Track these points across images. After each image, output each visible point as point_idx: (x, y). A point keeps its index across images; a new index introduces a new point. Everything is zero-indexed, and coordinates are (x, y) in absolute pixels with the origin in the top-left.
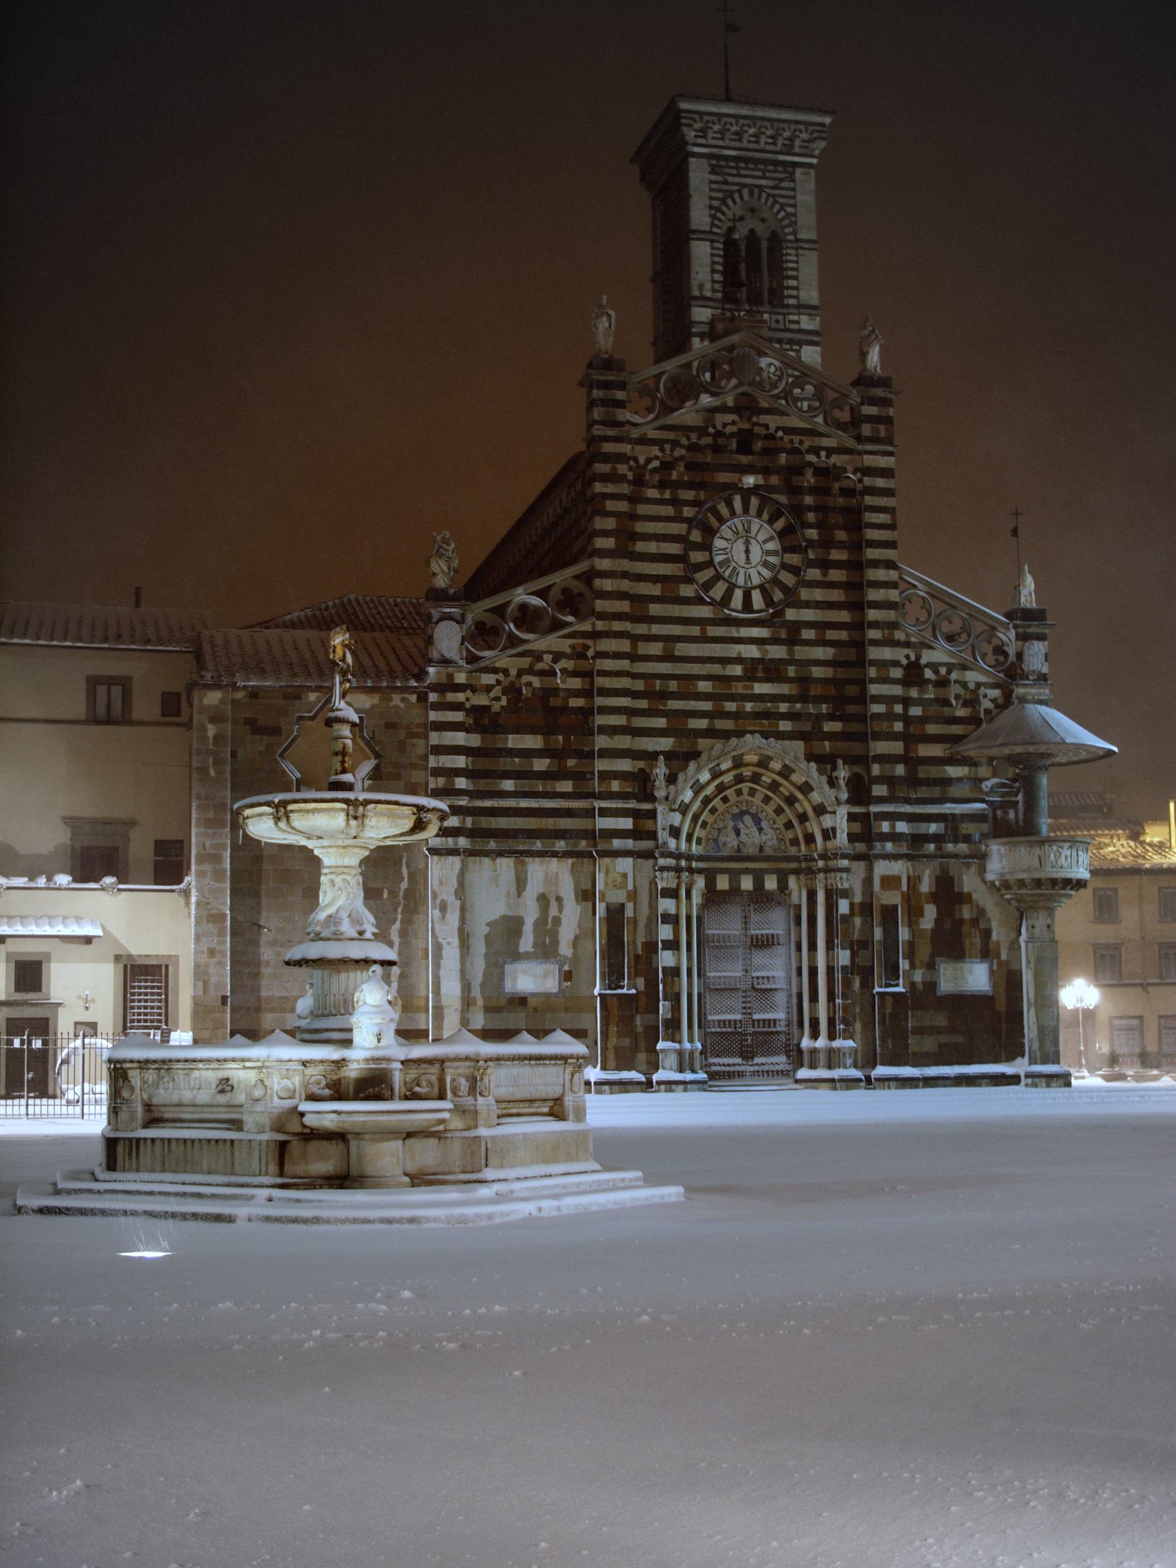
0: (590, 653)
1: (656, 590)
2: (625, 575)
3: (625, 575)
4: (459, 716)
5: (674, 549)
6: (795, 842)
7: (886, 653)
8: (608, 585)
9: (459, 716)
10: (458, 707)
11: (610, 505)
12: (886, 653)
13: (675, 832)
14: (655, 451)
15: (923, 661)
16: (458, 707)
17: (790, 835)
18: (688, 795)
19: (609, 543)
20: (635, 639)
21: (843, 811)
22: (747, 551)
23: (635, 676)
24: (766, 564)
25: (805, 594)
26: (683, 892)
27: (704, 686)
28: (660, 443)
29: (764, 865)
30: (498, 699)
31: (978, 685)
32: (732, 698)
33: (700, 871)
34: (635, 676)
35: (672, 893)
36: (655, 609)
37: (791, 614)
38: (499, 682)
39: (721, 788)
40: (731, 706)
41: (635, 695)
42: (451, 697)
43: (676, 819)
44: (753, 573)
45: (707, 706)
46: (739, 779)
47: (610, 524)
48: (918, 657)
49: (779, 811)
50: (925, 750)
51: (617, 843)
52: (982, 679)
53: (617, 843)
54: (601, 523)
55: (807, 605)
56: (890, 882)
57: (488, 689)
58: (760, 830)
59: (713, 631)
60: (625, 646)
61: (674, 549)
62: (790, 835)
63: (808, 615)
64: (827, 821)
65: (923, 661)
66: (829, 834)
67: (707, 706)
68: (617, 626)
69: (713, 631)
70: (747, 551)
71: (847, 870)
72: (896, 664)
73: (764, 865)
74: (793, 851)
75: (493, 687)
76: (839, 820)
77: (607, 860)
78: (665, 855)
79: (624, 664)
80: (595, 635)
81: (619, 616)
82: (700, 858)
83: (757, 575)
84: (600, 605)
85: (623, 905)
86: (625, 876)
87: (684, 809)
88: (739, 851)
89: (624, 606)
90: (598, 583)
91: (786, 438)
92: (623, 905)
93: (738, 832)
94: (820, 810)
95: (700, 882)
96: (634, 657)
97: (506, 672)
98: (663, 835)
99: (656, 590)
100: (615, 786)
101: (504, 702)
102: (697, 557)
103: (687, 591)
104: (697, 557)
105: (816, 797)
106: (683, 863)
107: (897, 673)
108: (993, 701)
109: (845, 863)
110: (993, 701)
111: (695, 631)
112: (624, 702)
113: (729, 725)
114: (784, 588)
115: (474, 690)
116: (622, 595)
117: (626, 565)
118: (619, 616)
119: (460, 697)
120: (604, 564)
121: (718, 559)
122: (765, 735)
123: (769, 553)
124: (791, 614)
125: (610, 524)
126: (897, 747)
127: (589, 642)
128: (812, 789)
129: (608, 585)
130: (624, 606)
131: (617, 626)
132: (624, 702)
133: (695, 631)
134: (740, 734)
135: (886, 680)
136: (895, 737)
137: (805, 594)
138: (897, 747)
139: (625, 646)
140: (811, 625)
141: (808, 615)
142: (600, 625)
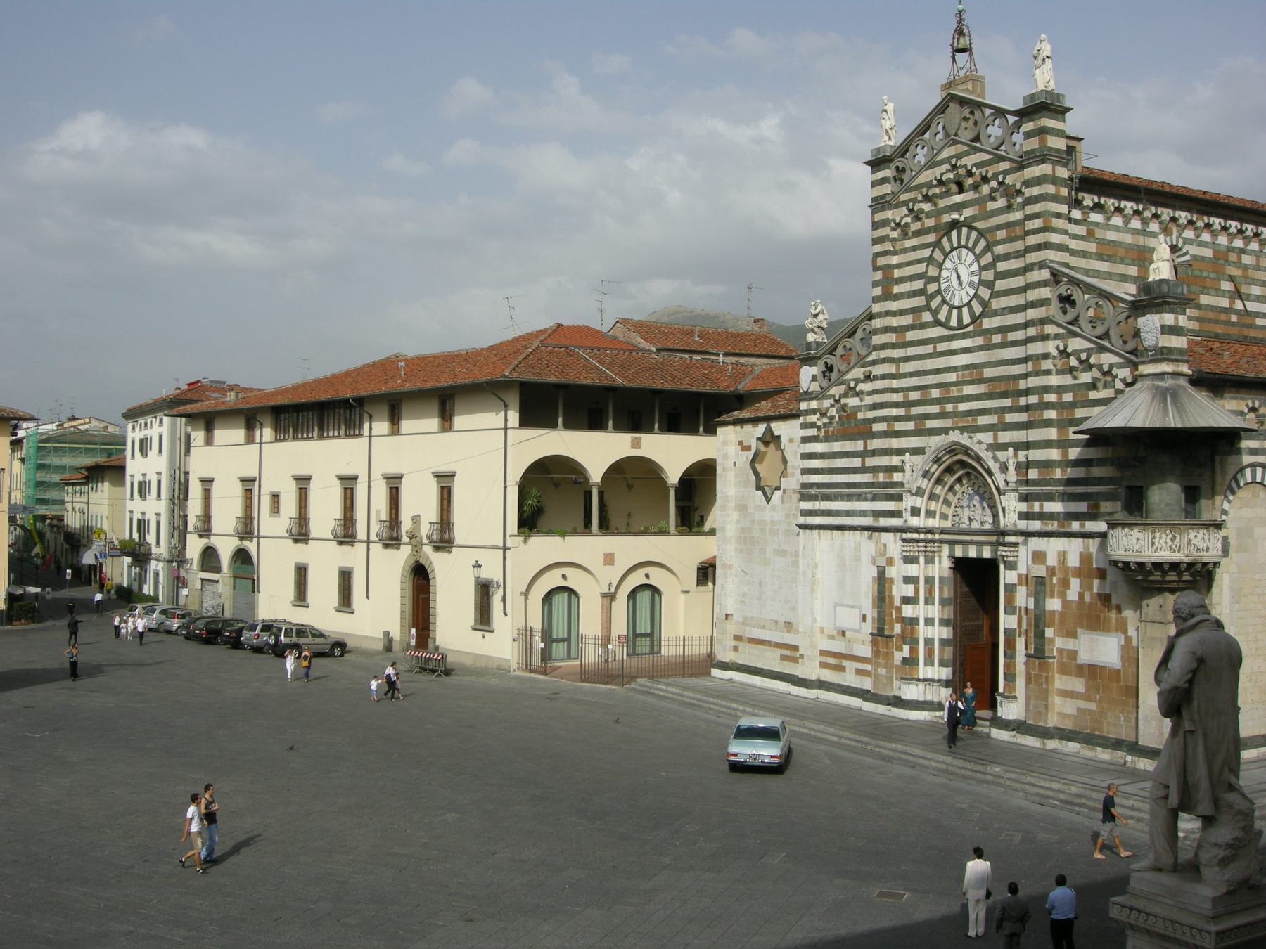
5: (918, 285)
13: (915, 512)
25: (996, 304)
31: (1111, 366)
36: (910, 336)
37: (987, 323)
40: (949, 408)
41: (897, 405)
59: (942, 347)
61: (918, 285)
69: (942, 347)
71: (1016, 545)
72: (1046, 356)
83: (965, 295)
87: (919, 492)
103: (927, 317)
108: (1123, 381)
110: (1123, 381)
111: (929, 349)
124: (987, 323)
133: (929, 349)
137: (996, 304)
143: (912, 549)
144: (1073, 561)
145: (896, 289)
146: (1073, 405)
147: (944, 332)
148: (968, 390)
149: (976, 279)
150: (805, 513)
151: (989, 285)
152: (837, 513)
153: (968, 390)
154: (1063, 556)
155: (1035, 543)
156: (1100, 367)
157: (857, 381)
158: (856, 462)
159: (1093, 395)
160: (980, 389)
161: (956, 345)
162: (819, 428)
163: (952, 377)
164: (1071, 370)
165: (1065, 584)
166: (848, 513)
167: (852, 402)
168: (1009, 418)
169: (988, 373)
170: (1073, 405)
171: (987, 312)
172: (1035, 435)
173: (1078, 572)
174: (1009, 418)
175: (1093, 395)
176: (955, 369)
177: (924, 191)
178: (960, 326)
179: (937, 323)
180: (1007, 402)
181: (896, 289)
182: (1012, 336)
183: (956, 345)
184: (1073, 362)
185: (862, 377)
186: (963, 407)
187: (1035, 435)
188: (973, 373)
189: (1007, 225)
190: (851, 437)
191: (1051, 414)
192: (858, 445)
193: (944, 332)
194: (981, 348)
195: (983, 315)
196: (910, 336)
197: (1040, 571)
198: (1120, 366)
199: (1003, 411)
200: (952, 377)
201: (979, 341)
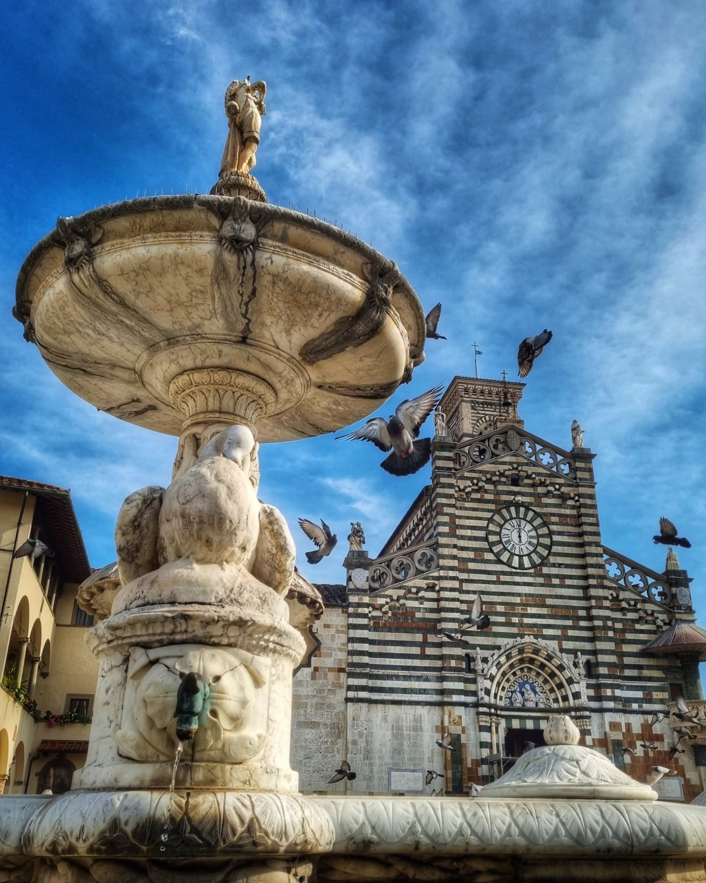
0: (437, 588)
1: (471, 555)
2: (455, 546)
3: (455, 546)
4: (365, 621)
5: (482, 534)
6: (556, 700)
7: (600, 592)
8: (446, 551)
9: (365, 621)
10: (365, 616)
11: (446, 510)
12: (600, 592)
13: (488, 692)
14: (469, 483)
15: (621, 597)
16: (365, 616)
17: (553, 696)
18: (494, 670)
19: (446, 529)
20: (462, 581)
21: (583, 683)
22: (520, 537)
23: (462, 602)
24: (530, 543)
25: (552, 559)
26: (494, 729)
27: (500, 609)
28: (471, 479)
29: (538, 714)
30: (386, 613)
32: (515, 615)
33: (503, 717)
34: (462, 602)
35: (488, 729)
36: (471, 566)
37: (545, 570)
38: (387, 603)
39: (512, 666)
40: (515, 620)
42: (360, 610)
43: (487, 684)
44: (523, 547)
45: (502, 619)
46: (522, 661)
47: (446, 519)
48: (618, 596)
49: (546, 681)
50: (626, 648)
51: (455, 698)
52: (655, 608)
53: (455, 698)
54: (441, 519)
55: (554, 565)
56: (615, 726)
57: (382, 606)
58: (536, 693)
59: (503, 578)
60: (456, 584)
61: (482, 534)
62: (553, 696)
63: (555, 571)
64: (576, 688)
65: (621, 597)
66: (577, 695)
67: (502, 619)
68: (451, 574)
69: (503, 578)
70: (520, 537)
71: (589, 717)
72: (606, 598)
73: (538, 714)
74: (555, 706)
75: (384, 605)
76: (581, 687)
77: (450, 707)
78: (483, 705)
79: (456, 595)
80: (440, 578)
81: (452, 568)
82: (502, 709)
83: (526, 549)
84: (442, 562)
85: (459, 735)
86: (460, 717)
87: (492, 678)
88: (524, 705)
89: (455, 563)
90: (441, 551)
91: (537, 478)
92: (459, 735)
93: (523, 694)
94: (570, 681)
95: (503, 723)
96: (461, 591)
97: (390, 597)
98: (482, 694)
99: (471, 555)
100: (453, 663)
101: (390, 614)
102: (492, 538)
103: (489, 556)
104: (492, 538)
105: (567, 673)
106: (493, 711)
107: (607, 603)
108: (663, 621)
109: (587, 713)
110: (663, 621)
111: (494, 578)
112: (456, 615)
113: (515, 630)
114: (540, 556)
115: (375, 609)
116: (454, 557)
117: (454, 541)
118: (452, 568)
119: (366, 610)
120: (443, 540)
121: (504, 540)
122: (536, 637)
123: (531, 537)
124: (545, 570)
125: (446, 519)
126: (611, 646)
127: (436, 582)
128: (564, 669)
129: (446, 551)
130: (455, 563)
131: (451, 574)
132: (456, 615)
133: (494, 578)
134: (522, 636)
135: (601, 608)
136: (610, 639)
137: (552, 559)
138: (611, 646)
139: (456, 584)
140: (557, 576)
141: (555, 571)
142: (442, 573)
143: (485, 720)
144: (636, 729)
145: (459, 532)
146: (624, 631)
147: (506, 569)
148: (530, 610)
149: (535, 541)
150: (350, 688)
151: (549, 548)
152: (392, 690)
153: (530, 610)
154: (628, 726)
155: (609, 717)
156: (645, 611)
157: (419, 589)
158: (416, 650)
159: (638, 626)
160: (544, 611)
161: (517, 579)
162: (369, 618)
163: (518, 600)
164: (622, 610)
165: (632, 745)
166: (405, 691)
167: (411, 604)
168: (571, 633)
169: (549, 601)
170: (624, 631)
171: (544, 562)
172: (601, 645)
173: (641, 737)
174: (571, 633)
175: (638, 626)
176: (519, 595)
177: (489, 476)
178: (521, 565)
179: (500, 562)
180: (569, 623)
181: (459, 532)
182: (568, 582)
183: (517, 579)
184: (624, 605)
185: (425, 587)
186: (526, 621)
187: (601, 645)
188: (540, 601)
189: (560, 515)
190: (397, 630)
191: (611, 634)
192: (419, 637)
193: (506, 569)
194: (542, 585)
195: (542, 564)
196: (471, 566)
197: (617, 736)
198: (660, 612)
199: (565, 628)
200: (518, 600)
201: (541, 580)
